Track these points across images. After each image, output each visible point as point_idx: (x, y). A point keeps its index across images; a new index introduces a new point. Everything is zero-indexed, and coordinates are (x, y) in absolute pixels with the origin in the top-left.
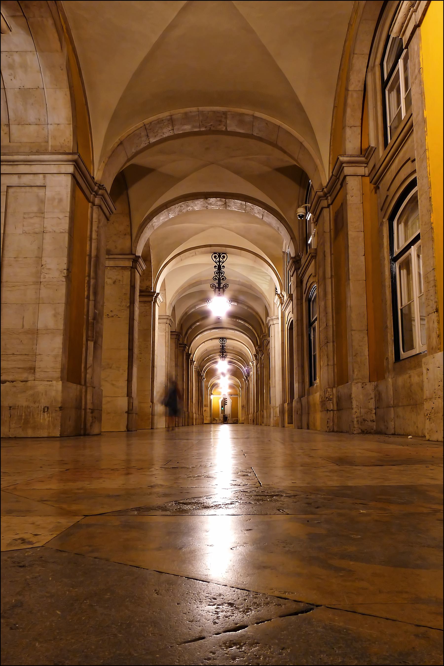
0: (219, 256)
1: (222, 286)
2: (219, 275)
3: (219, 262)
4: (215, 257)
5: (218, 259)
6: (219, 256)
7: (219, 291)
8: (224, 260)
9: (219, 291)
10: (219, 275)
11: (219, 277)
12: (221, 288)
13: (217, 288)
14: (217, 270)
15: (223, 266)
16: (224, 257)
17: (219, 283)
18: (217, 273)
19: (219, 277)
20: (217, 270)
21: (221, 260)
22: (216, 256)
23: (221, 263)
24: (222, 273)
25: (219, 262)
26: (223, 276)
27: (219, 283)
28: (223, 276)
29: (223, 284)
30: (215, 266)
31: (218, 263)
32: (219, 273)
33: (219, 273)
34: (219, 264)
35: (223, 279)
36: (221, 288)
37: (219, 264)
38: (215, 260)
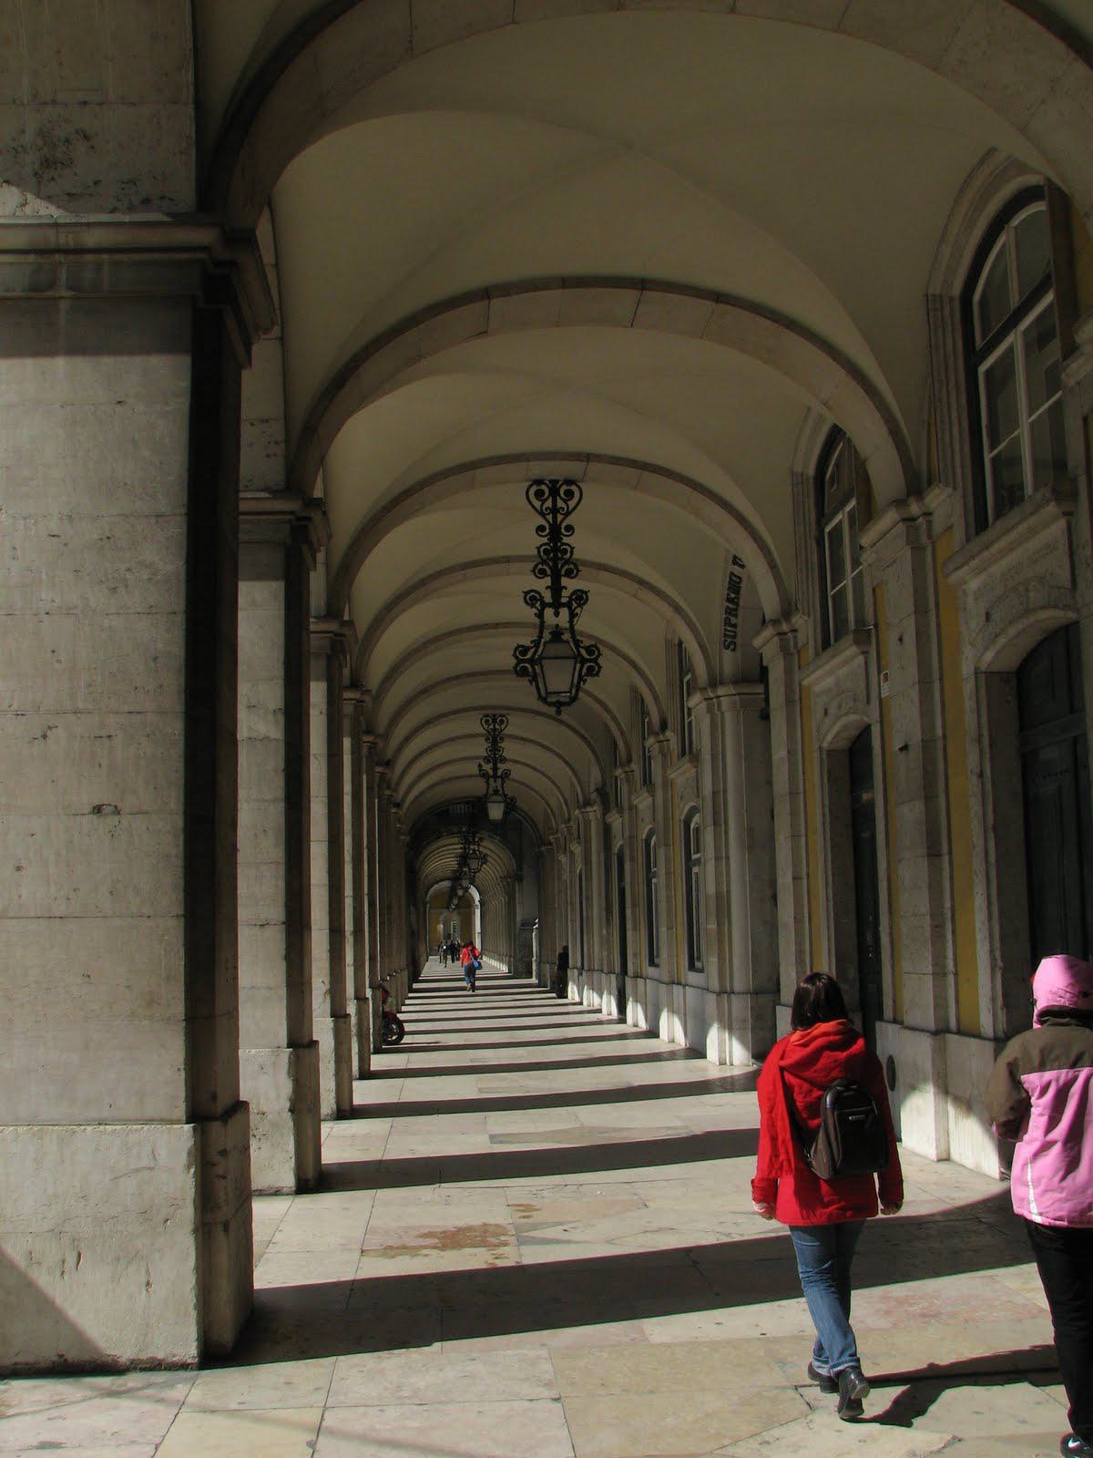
0: (554, 492)
1: (564, 600)
2: (555, 560)
3: (555, 510)
4: (539, 494)
5: (549, 503)
6: (554, 492)
7: (557, 614)
8: (572, 504)
9: (557, 614)
10: (555, 560)
11: (555, 563)
13: (549, 605)
14: (545, 540)
15: (570, 528)
16: (570, 494)
17: (556, 589)
20: (545, 540)
21: (560, 503)
22: (542, 492)
23: (560, 517)
25: (495, 729)
26: (567, 562)
27: (556, 589)
29: (570, 590)
30: (540, 529)
31: (550, 517)
32: (556, 549)
33: (556, 549)
34: (555, 518)
36: (564, 605)
37: (555, 518)
38: (537, 504)
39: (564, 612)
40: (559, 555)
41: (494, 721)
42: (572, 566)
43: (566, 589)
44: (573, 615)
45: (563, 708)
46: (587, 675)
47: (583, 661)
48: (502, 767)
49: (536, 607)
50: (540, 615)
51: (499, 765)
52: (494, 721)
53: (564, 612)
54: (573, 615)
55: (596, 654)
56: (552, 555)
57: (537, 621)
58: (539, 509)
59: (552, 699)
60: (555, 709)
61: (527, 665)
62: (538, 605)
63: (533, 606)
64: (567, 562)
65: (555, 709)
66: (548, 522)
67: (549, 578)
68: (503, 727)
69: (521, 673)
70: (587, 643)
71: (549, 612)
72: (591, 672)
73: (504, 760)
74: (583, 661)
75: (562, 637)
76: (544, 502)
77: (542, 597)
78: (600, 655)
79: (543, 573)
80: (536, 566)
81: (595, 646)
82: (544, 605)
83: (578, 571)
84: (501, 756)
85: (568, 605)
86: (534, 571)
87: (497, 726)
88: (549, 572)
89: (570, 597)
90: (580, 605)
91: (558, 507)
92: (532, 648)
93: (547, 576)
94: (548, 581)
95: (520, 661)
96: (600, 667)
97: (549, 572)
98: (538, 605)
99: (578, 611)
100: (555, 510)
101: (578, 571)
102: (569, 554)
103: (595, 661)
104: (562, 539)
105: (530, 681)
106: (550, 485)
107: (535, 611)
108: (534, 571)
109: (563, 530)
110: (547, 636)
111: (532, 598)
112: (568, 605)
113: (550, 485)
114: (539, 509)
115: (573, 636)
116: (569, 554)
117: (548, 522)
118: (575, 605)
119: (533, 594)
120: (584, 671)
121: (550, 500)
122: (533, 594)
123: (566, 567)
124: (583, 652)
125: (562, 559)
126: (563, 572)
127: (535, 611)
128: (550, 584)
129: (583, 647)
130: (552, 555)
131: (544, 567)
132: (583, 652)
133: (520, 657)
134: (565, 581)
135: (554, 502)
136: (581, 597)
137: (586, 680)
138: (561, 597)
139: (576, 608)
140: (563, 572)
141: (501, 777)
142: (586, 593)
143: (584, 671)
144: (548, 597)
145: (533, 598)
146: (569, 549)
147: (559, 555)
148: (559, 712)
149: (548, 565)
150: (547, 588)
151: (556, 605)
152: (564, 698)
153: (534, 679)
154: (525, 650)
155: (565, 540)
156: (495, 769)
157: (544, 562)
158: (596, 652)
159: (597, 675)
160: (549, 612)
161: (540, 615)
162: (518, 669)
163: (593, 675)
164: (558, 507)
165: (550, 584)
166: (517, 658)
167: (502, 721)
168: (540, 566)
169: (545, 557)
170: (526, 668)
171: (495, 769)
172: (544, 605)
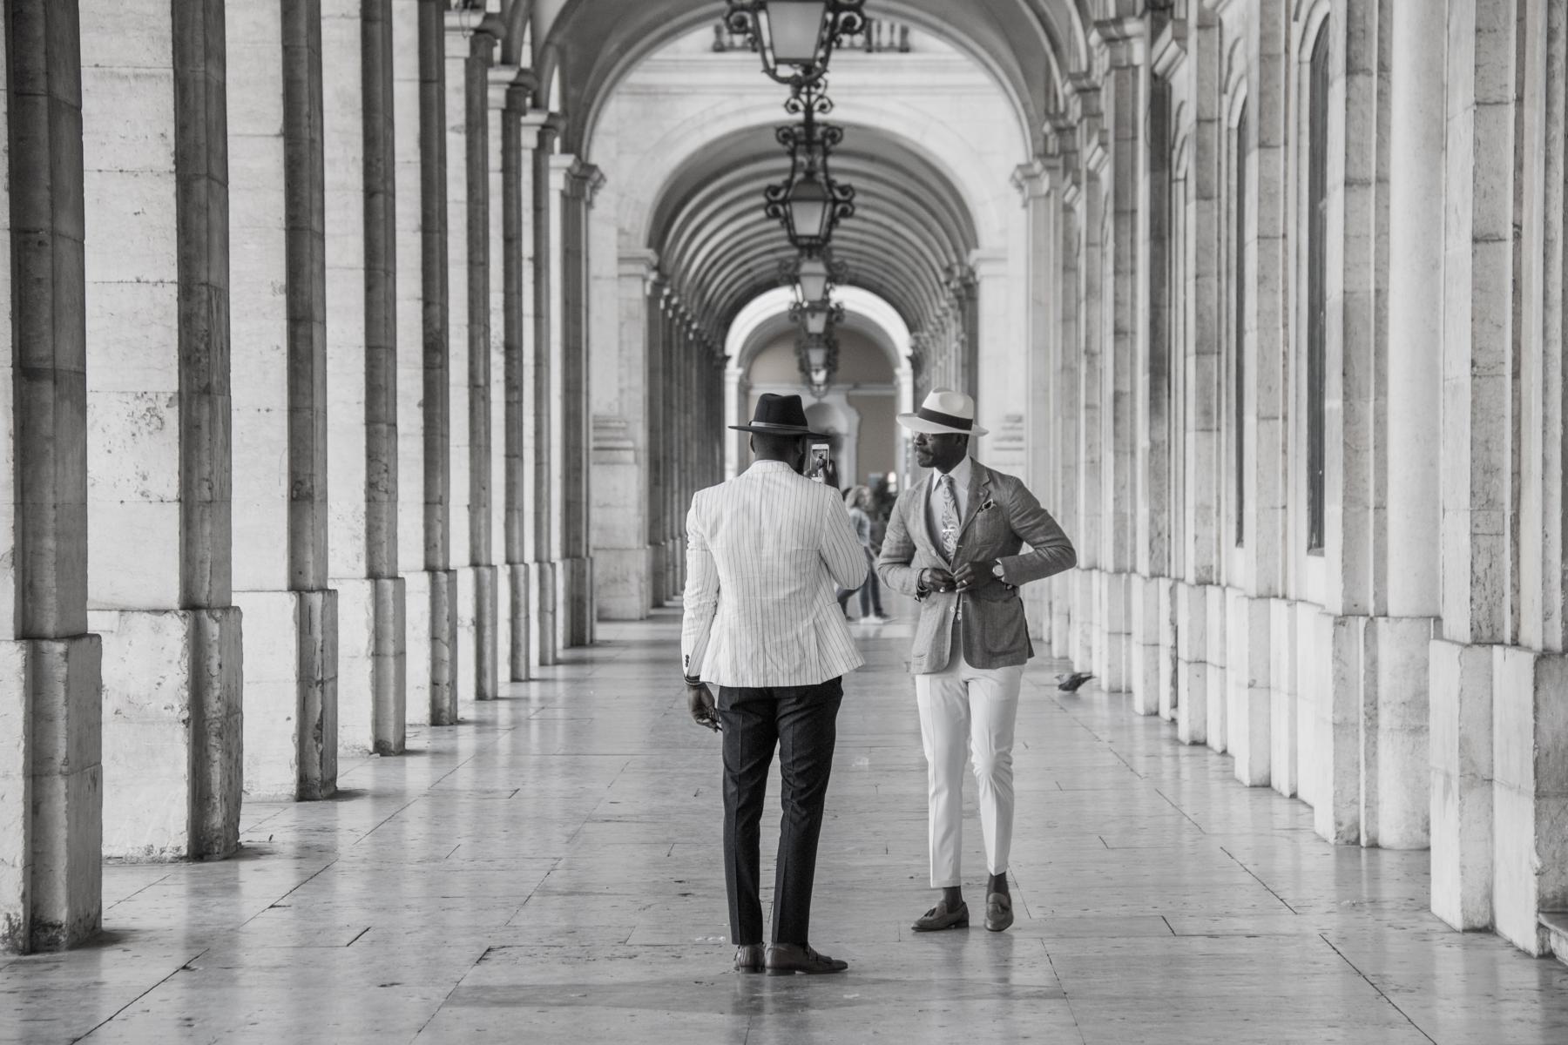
12: (818, 143)
26: (821, 97)
28: (821, 97)
35: (823, 107)
47: (835, 202)
51: (818, 116)
63: (785, 143)
79: (795, 108)
90: (834, 143)
94: (800, 116)
103: (849, 202)
118: (828, 142)
124: (838, 195)
132: (838, 195)
141: (822, 143)
145: (785, 136)
154: (774, 190)
160: (801, 147)
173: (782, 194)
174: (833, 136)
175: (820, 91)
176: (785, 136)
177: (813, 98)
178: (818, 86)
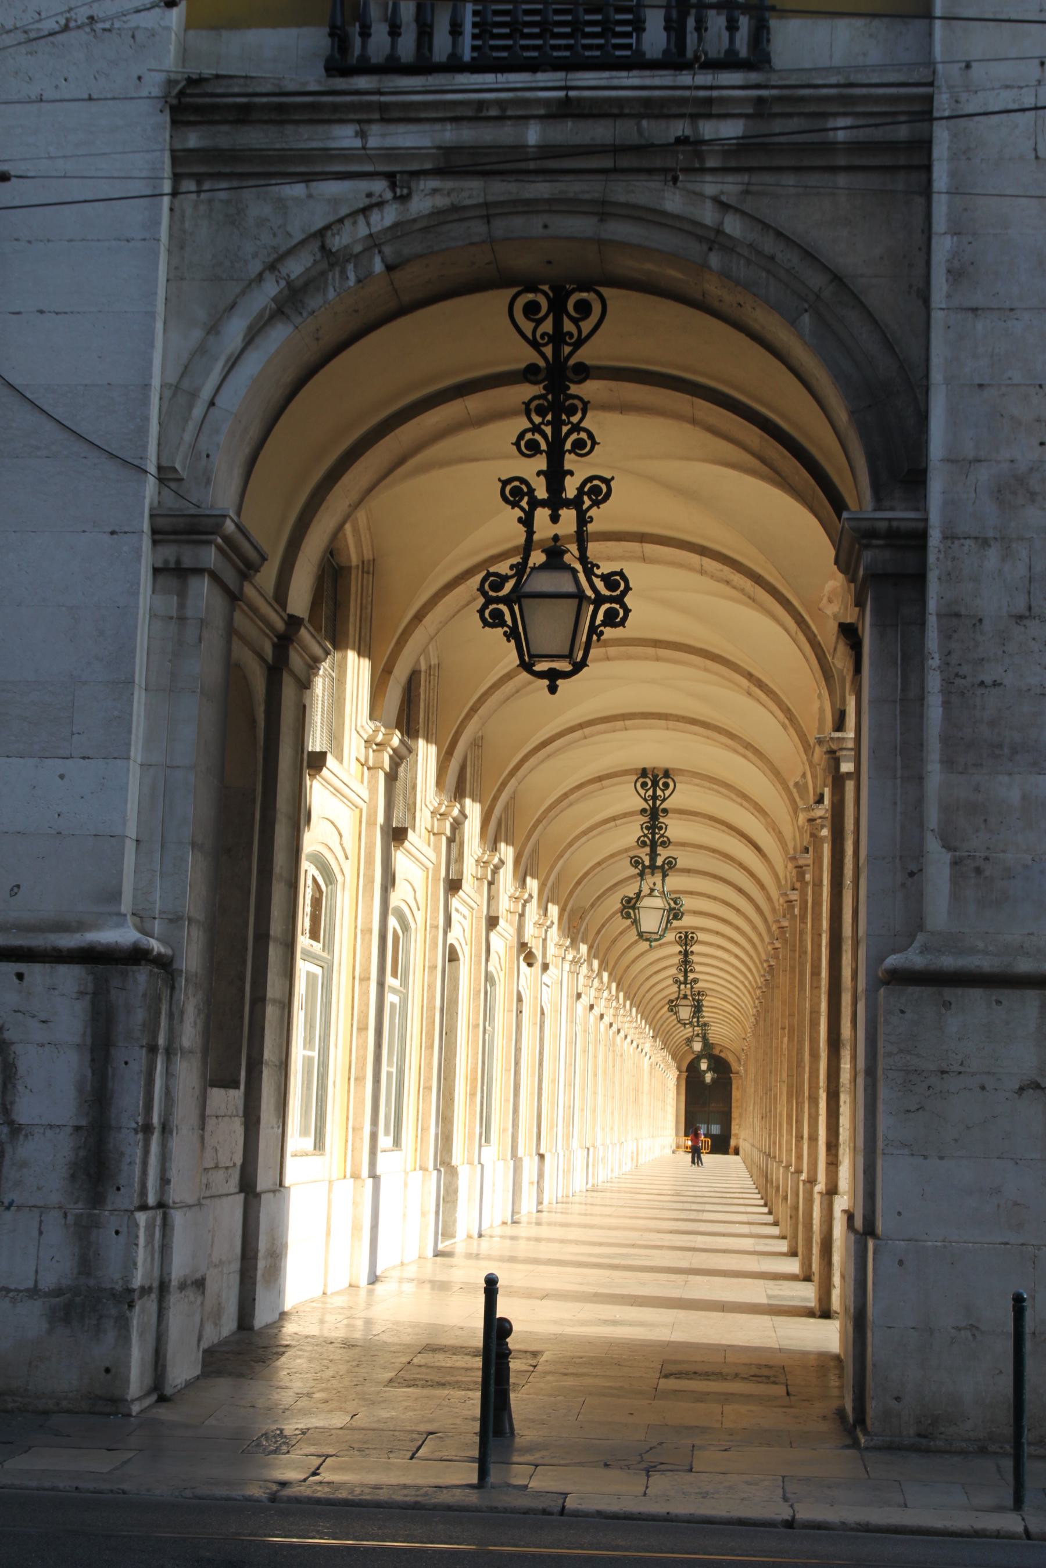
1: (571, 492)
2: (556, 425)
3: (558, 337)
4: (531, 309)
5: (547, 326)
7: (555, 518)
8: (586, 326)
9: (555, 518)
13: (543, 503)
16: (584, 308)
17: (555, 475)
18: (541, 411)
19: (557, 431)
24: (573, 411)
26: (576, 428)
27: (555, 475)
31: (548, 350)
34: (556, 352)
35: (579, 444)
36: (568, 503)
38: (527, 327)
39: (568, 515)
40: (564, 417)
41: (655, 784)
42: (583, 435)
43: (571, 473)
44: (582, 520)
45: (559, 682)
46: (604, 623)
47: (599, 600)
48: (663, 854)
49: (522, 509)
50: (527, 522)
52: (655, 784)
53: (568, 515)
54: (582, 520)
55: (622, 587)
56: (549, 417)
57: (522, 529)
58: (530, 336)
59: (542, 666)
60: (546, 682)
61: (502, 607)
62: (524, 503)
63: (515, 504)
64: (576, 428)
65: (546, 682)
66: (543, 355)
67: (544, 454)
68: (667, 793)
69: (496, 620)
70: (605, 568)
71: (542, 515)
72: (611, 619)
73: (666, 844)
74: (599, 600)
75: (567, 558)
76: (539, 322)
77: (531, 491)
78: (628, 588)
79: (533, 448)
80: (521, 436)
81: (621, 574)
82: (535, 503)
83: (594, 443)
84: (662, 836)
85: (576, 503)
86: (517, 444)
87: (659, 792)
88: (544, 446)
89: (580, 489)
90: (596, 503)
91: (565, 330)
92: (512, 577)
93: (541, 452)
94: (541, 463)
95: (489, 601)
96: (627, 611)
97: (544, 446)
98: (524, 503)
99: (588, 514)
100: (558, 337)
101: (594, 443)
102: (579, 415)
103: (620, 600)
104: (568, 388)
105: (505, 633)
106: (551, 295)
107: (518, 513)
108: (517, 444)
109: (570, 375)
110: (538, 558)
111: (515, 492)
112: (576, 503)
113: (551, 295)
114: (530, 336)
115: (583, 559)
116: (579, 415)
117: (543, 355)
118: (587, 503)
119: (517, 483)
120: (600, 617)
121: (550, 321)
122: (517, 483)
123: (574, 436)
125: (564, 423)
126: (568, 446)
127: (518, 513)
128: (544, 467)
129: (597, 576)
130: (549, 417)
131: (538, 437)
132: (600, 585)
133: (491, 593)
134: (570, 461)
135: (558, 324)
136: (598, 491)
137: (602, 633)
138: (563, 489)
139: (589, 508)
140: (568, 446)
142: (607, 482)
143: (600, 617)
144: (542, 493)
146: (580, 405)
147: (564, 417)
148: (553, 689)
149: (544, 435)
150: (539, 474)
151: (556, 502)
152: (564, 666)
153: (513, 634)
155: (574, 389)
156: (653, 855)
157: (536, 429)
158: (622, 587)
159: (622, 623)
160: (542, 515)
161: (527, 522)
162: (487, 612)
163: (615, 625)
164: (565, 330)
165: (544, 467)
166: (484, 594)
167: (666, 786)
168: (529, 436)
169: (537, 420)
170: (501, 614)
171: (653, 855)
172: (535, 503)
173: (509, 586)
174: (596, 490)
175: (662, 832)
176: (517, 492)
177: (565, 429)
178: (661, 828)
